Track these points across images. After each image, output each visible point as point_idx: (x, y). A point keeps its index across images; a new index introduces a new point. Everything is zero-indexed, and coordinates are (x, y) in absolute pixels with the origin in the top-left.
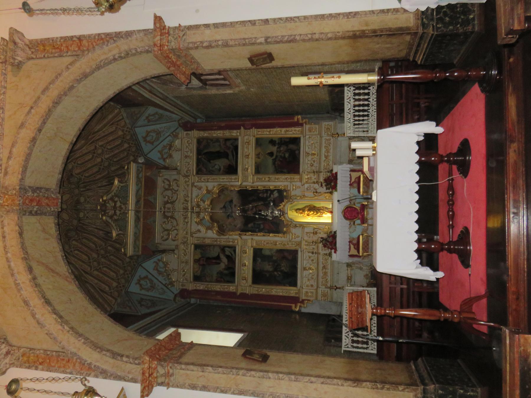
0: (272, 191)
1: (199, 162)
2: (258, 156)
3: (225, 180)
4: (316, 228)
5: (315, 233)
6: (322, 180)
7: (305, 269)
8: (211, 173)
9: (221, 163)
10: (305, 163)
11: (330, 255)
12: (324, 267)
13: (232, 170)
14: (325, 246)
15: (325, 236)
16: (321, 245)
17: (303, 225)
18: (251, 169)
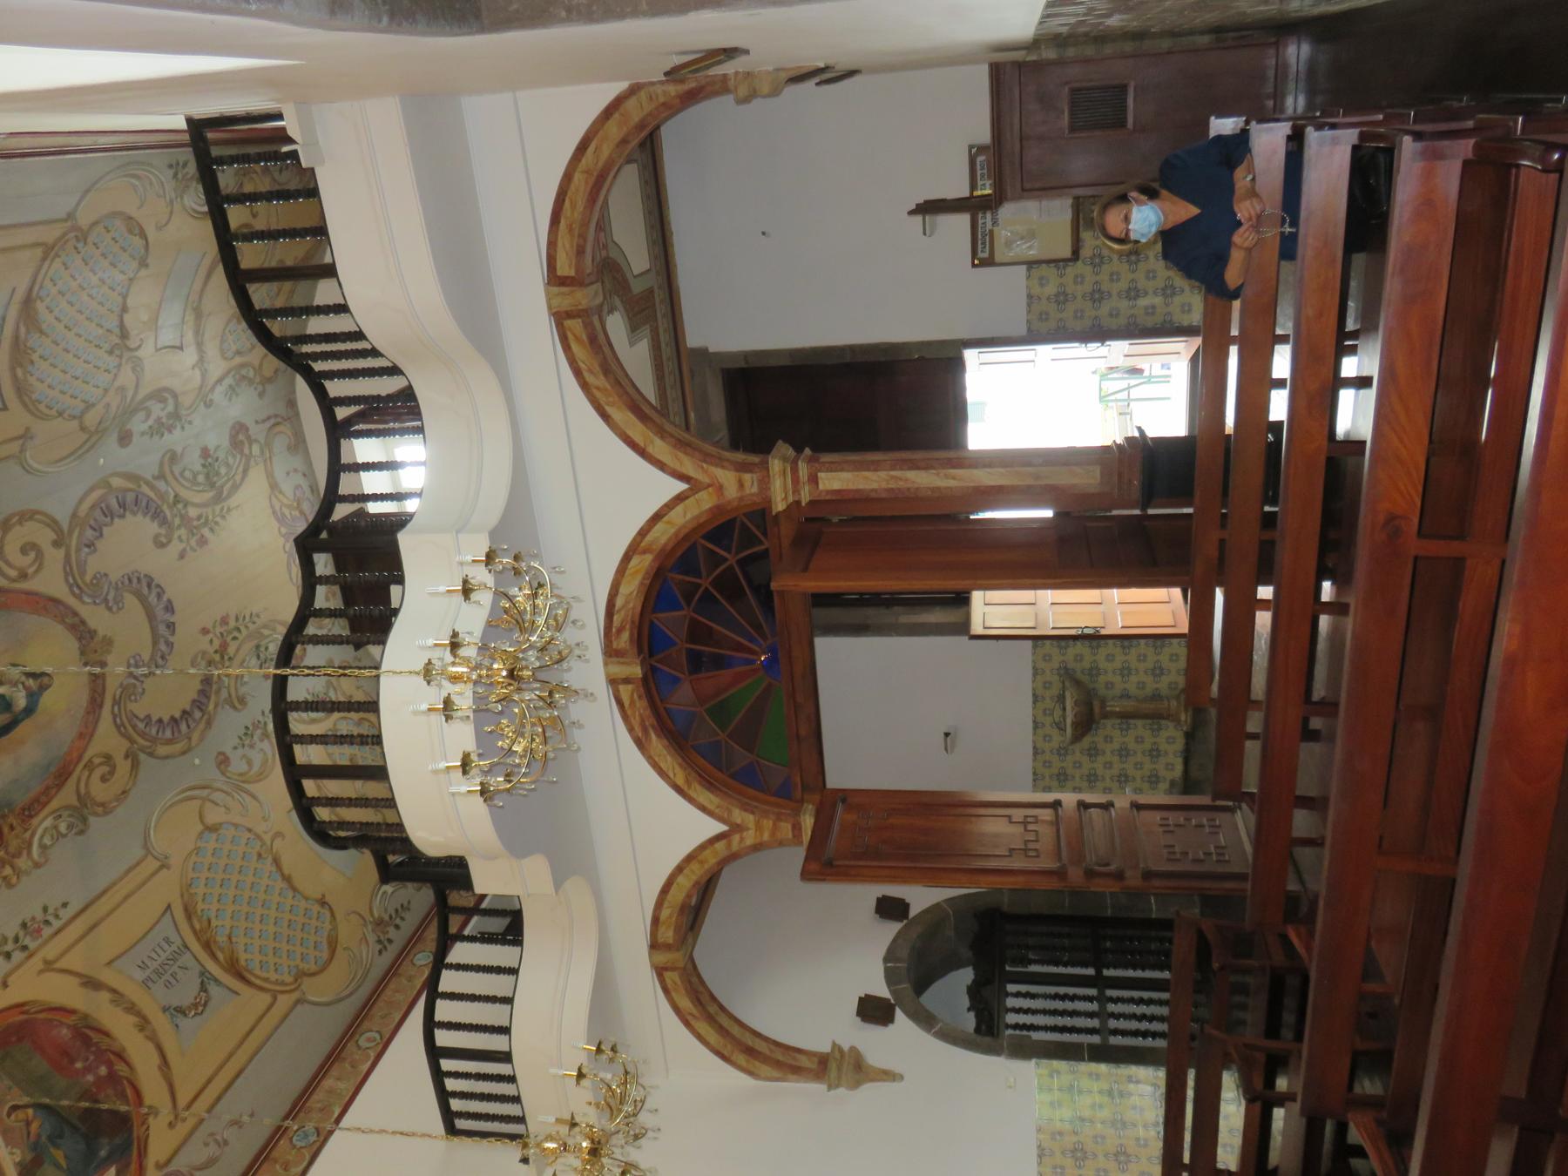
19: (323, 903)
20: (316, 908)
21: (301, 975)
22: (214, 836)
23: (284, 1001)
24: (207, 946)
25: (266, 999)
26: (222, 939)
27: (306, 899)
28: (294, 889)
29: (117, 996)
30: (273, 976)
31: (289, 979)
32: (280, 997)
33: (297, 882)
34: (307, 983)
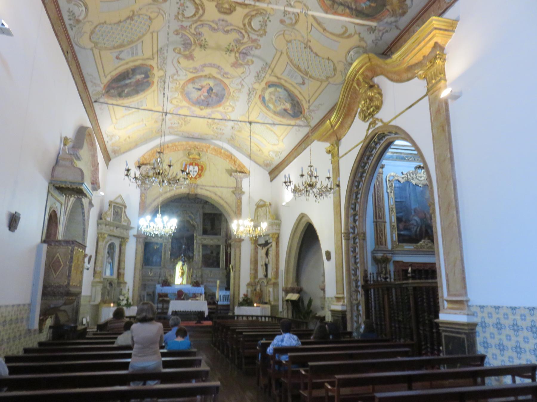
0: (193, 253)
1: (210, 214)
2: (212, 246)
3: (200, 229)
4: (173, 276)
5: (170, 275)
6: (198, 279)
7: (151, 270)
8: (204, 220)
9: (209, 227)
10: (207, 271)
11: (159, 283)
12: (152, 280)
13: (205, 232)
14: (164, 281)
15: (169, 281)
16: (164, 278)
17: (174, 268)
18: (205, 242)
19: (328, 59)
20: (327, 61)
21: (328, 78)
22: (290, 44)
23: (325, 84)
24: (300, 70)
25: (318, 83)
26: (303, 69)
27: (323, 58)
28: (319, 56)
29: (286, 81)
30: (320, 78)
31: (324, 78)
32: (323, 83)
33: (319, 54)
34: (330, 80)
